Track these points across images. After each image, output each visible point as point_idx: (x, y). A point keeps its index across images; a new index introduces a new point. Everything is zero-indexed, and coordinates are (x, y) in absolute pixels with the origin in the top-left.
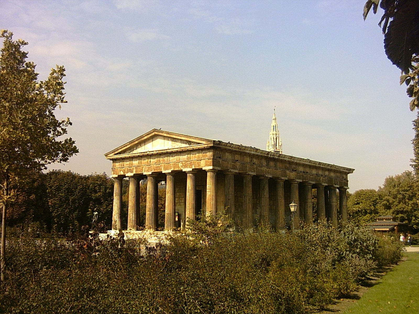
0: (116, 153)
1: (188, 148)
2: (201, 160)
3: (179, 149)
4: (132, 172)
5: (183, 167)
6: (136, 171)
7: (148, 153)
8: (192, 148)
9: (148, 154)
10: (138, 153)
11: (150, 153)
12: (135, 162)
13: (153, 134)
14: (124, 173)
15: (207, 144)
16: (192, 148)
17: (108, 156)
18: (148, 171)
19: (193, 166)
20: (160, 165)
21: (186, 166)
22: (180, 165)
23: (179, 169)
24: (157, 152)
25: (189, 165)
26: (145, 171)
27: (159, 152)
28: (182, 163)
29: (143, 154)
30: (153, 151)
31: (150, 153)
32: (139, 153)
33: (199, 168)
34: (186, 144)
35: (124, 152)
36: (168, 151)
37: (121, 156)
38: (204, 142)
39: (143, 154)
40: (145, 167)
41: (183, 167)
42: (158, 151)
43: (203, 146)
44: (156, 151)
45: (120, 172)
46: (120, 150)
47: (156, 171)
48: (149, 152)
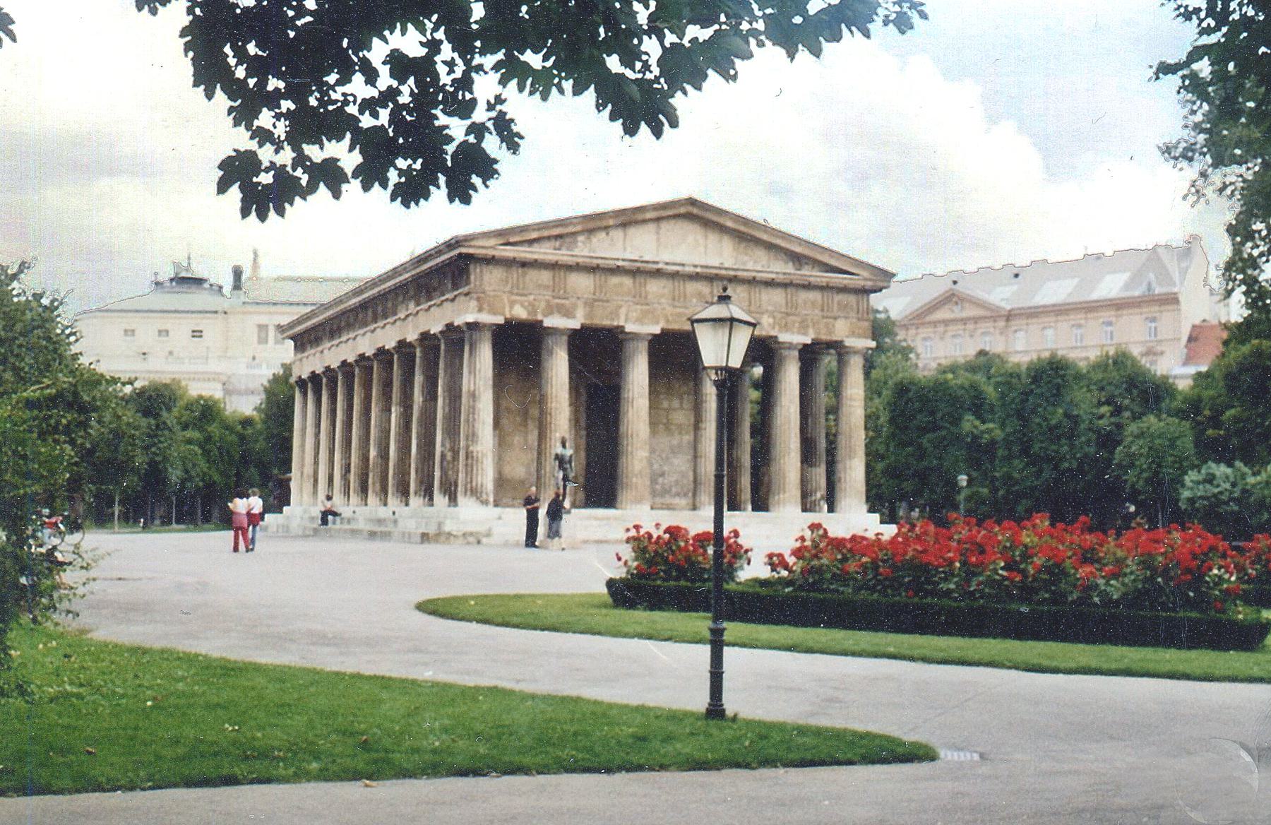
0: (512, 240)
1: (812, 279)
2: (835, 318)
3: (781, 276)
4: (568, 314)
6: (589, 315)
7: (660, 266)
12: (582, 283)
13: (682, 210)
17: (472, 243)
18: (639, 320)
21: (786, 328)
24: (699, 270)
26: (626, 321)
35: (531, 242)
37: (535, 257)
38: (865, 274)
44: (695, 266)
46: (534, 235)
48: (667, 264)
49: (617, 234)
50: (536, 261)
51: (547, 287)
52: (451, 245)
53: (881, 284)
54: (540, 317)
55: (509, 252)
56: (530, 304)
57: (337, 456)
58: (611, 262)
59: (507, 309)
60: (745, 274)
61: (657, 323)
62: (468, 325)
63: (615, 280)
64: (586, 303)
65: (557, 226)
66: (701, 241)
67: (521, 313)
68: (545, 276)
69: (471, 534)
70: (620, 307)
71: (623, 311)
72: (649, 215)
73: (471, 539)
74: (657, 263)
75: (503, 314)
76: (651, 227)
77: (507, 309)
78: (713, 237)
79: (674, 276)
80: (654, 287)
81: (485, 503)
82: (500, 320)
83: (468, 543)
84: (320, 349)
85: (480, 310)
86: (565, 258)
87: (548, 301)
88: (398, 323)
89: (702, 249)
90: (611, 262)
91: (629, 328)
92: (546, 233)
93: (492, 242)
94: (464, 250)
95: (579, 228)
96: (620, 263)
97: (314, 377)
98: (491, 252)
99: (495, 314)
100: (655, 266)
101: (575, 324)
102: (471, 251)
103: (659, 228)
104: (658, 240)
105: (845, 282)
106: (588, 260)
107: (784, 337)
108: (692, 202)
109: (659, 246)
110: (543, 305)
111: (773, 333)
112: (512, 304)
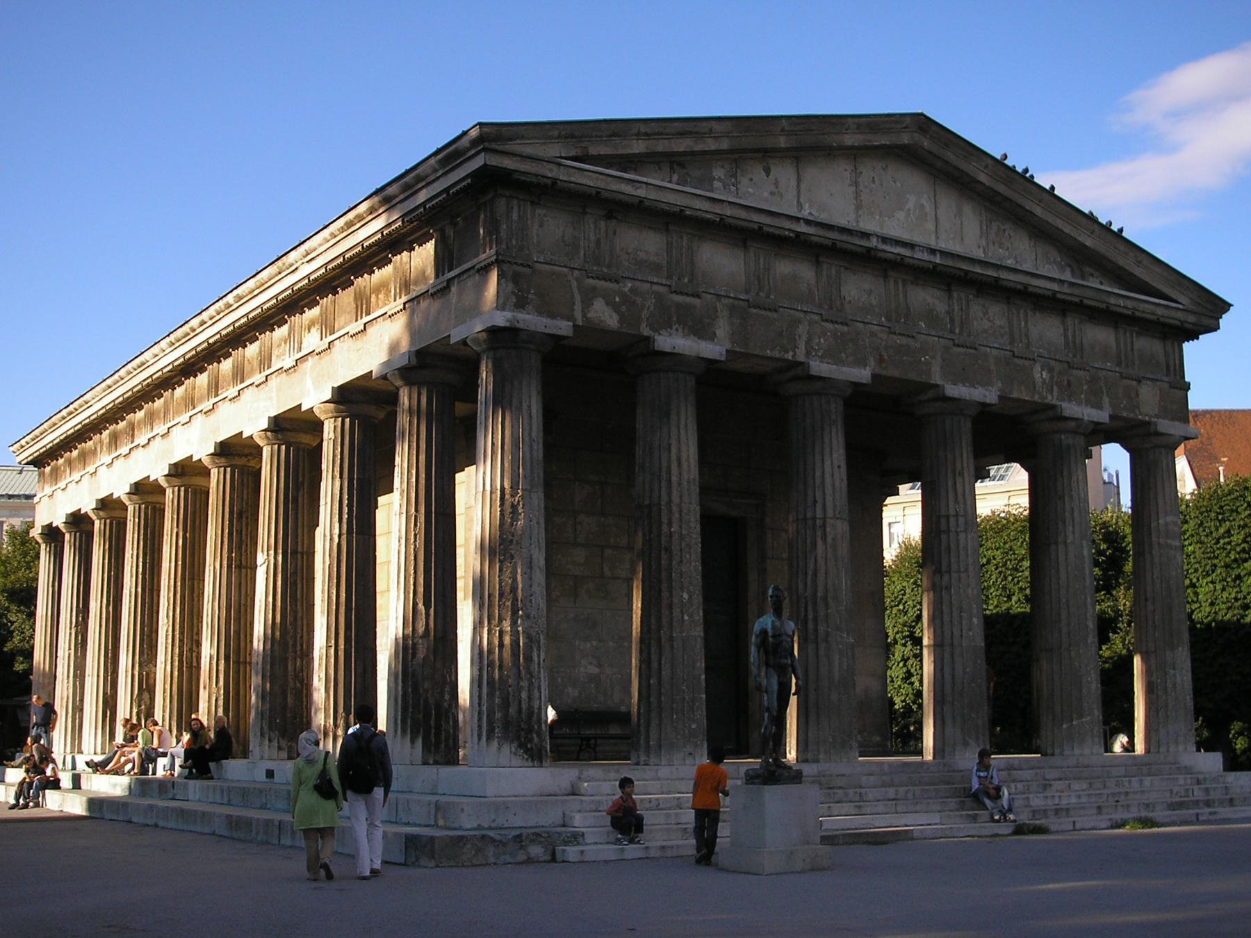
0: (593, 151)
1: (1113, 301)
2: (1139, 381)
3: (1066, 289)
4: (702, 330)
5: (1055, 388)
7: (874, 242)
8: (1130, 304)
9: (869, 249)
10: (798, 219)
11: (888, 248)
13: (905, 139)
14: (622, 319)
15: (1195, 313)
16: (1130, 304)
17: (509, 147)
18: (831, 355)
19: (1106, 400)
20: (918, 345)
21: (1069, 391)
22: (1040, 374)
23: (1036, 398)
25: (1085, 387)
26: (808, 353)
27: (950, 263)
28: (1051, 370)
29: (834, 235)
30: (912, 246)
31: (888, 248)
32: (808, 222)
33: (1132, 415)
34: (1062, 269)
36: (1003, 275)
37: (641, 192)
39: (834, 235)
40: (811, 323)
41: (1055, 388)
42: (943, 253)
43: (1180, 315)
44: (933, 251)
45: (587, 304)
46: (638, 147)
47: (895, 373)
48: (885, 240)
49: (784, 173)
50: (641, 201)
51: (656, 268)
52: (450, 155)
53: (1206, 321)
54: (646, 332)
55: (590, 177)
56: (624, 296)
57: (125, 660)
58: (787, 224)
59: (578, 308)
60: (1012, 277)
61: (862, 363)
62: (493, 331)
63: (785, 267)
64: (732, 309)
65: (682, 134)
66: (929, 208)
67: (604, 315)
68: (646, 243)
69: (536, 837)
70: (800, 322)
71: (802, 330)
72: (850, 140)
73: (536, 850)
74: (866, 235)
75: (570, 317)
76: (843, 168)
77: (578, 308)
78: (948, 203)
79: (898, 265)
80: (858, 289)
81: (535, 756)
82: (563, 327)
83: (530, 861)
84: (91, 469)
85: (521, 304)
86: (698, 204)
87: (659, 297)
88: (274, 381)
89: (930, 226)
90: (787, 224)
91: (819, 367)
92: (661, 146)
93: (554, 150)
94: (494, 161)
95: (724, 145)
96: (802, 228)
97: (78, 521)
98: (550, 172)
99: (552, 316)
100: (864, 243)
101: (712, 350)
102: (508, 163)
103: (856, 173)
104: (857, 195)
105: (1160, 311)
106: (743, 214)
107: (1071, 409)
108: (922, 123)
109: (858, 207)
110: (650, 303)
111: (1051, 399)
112: (589, 296)
